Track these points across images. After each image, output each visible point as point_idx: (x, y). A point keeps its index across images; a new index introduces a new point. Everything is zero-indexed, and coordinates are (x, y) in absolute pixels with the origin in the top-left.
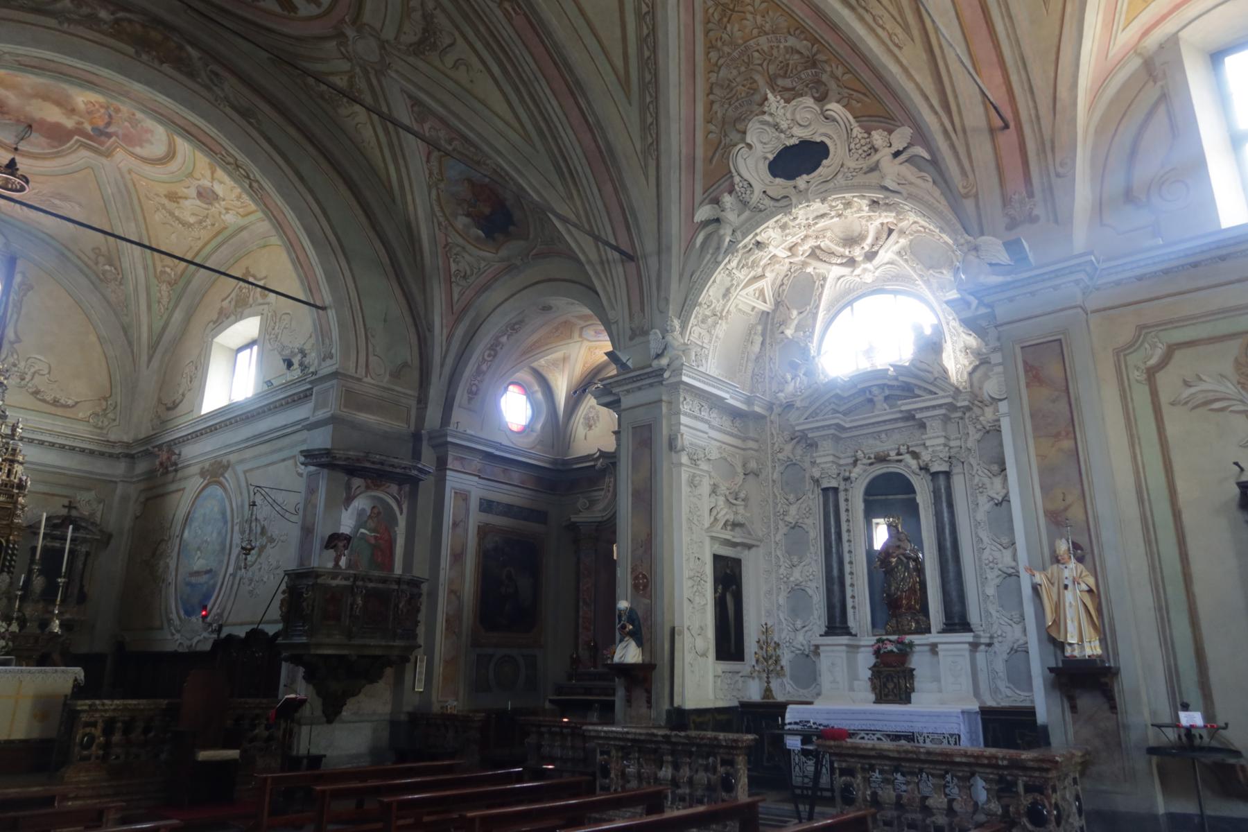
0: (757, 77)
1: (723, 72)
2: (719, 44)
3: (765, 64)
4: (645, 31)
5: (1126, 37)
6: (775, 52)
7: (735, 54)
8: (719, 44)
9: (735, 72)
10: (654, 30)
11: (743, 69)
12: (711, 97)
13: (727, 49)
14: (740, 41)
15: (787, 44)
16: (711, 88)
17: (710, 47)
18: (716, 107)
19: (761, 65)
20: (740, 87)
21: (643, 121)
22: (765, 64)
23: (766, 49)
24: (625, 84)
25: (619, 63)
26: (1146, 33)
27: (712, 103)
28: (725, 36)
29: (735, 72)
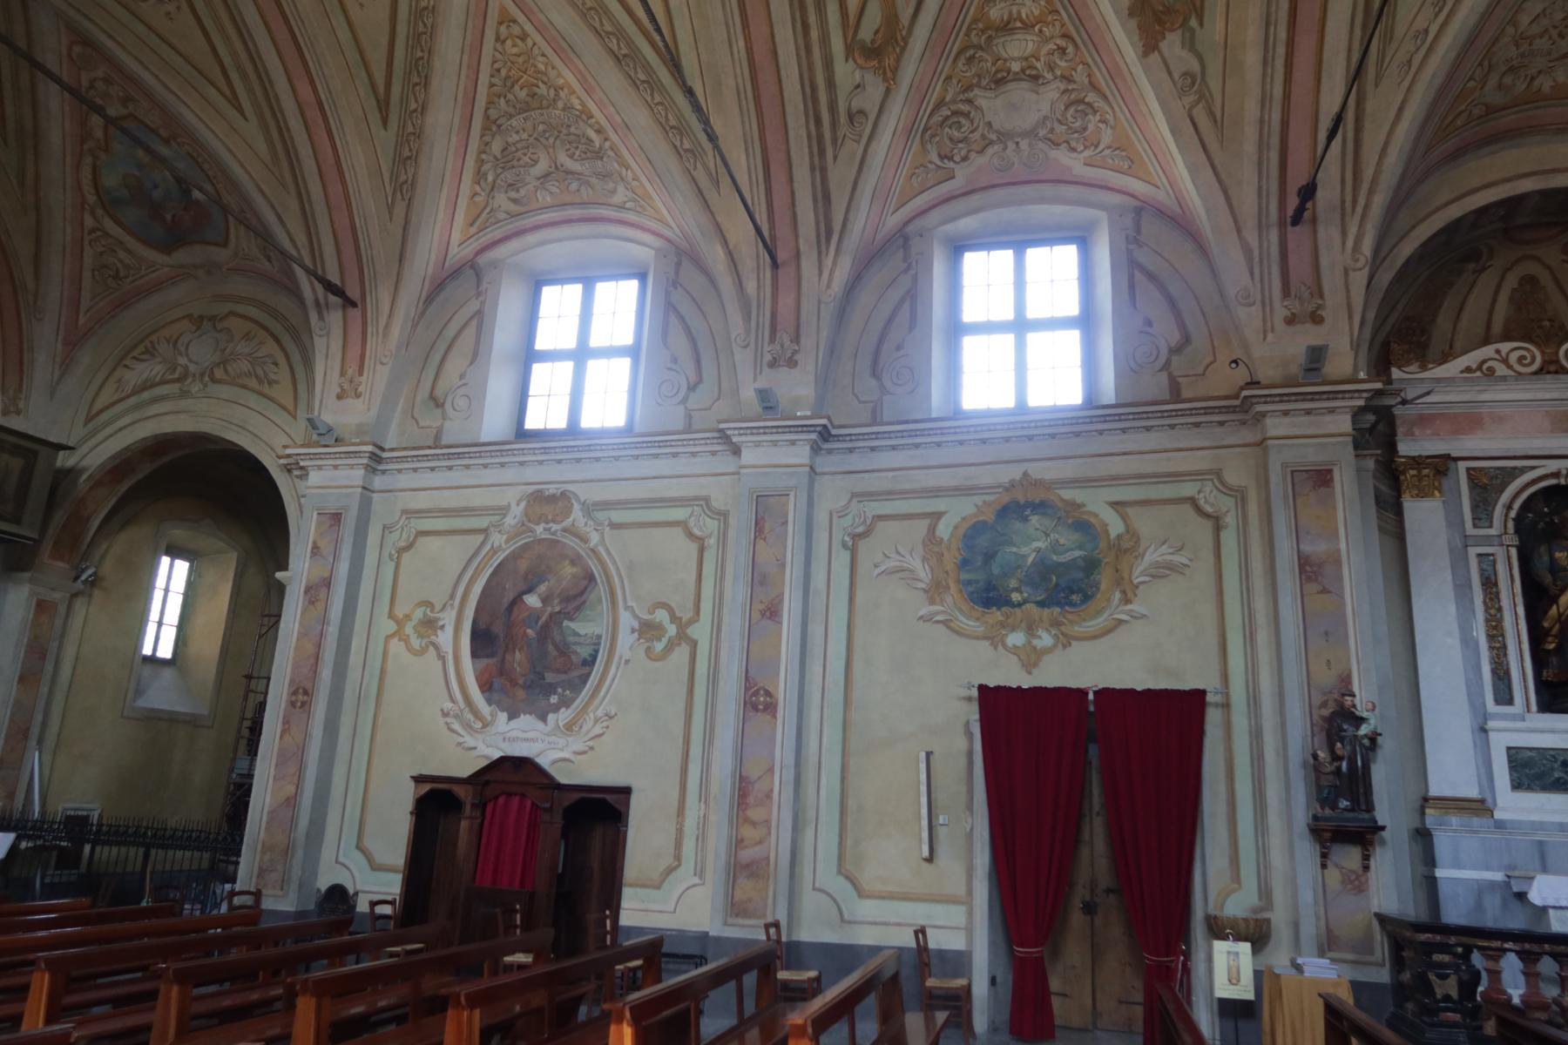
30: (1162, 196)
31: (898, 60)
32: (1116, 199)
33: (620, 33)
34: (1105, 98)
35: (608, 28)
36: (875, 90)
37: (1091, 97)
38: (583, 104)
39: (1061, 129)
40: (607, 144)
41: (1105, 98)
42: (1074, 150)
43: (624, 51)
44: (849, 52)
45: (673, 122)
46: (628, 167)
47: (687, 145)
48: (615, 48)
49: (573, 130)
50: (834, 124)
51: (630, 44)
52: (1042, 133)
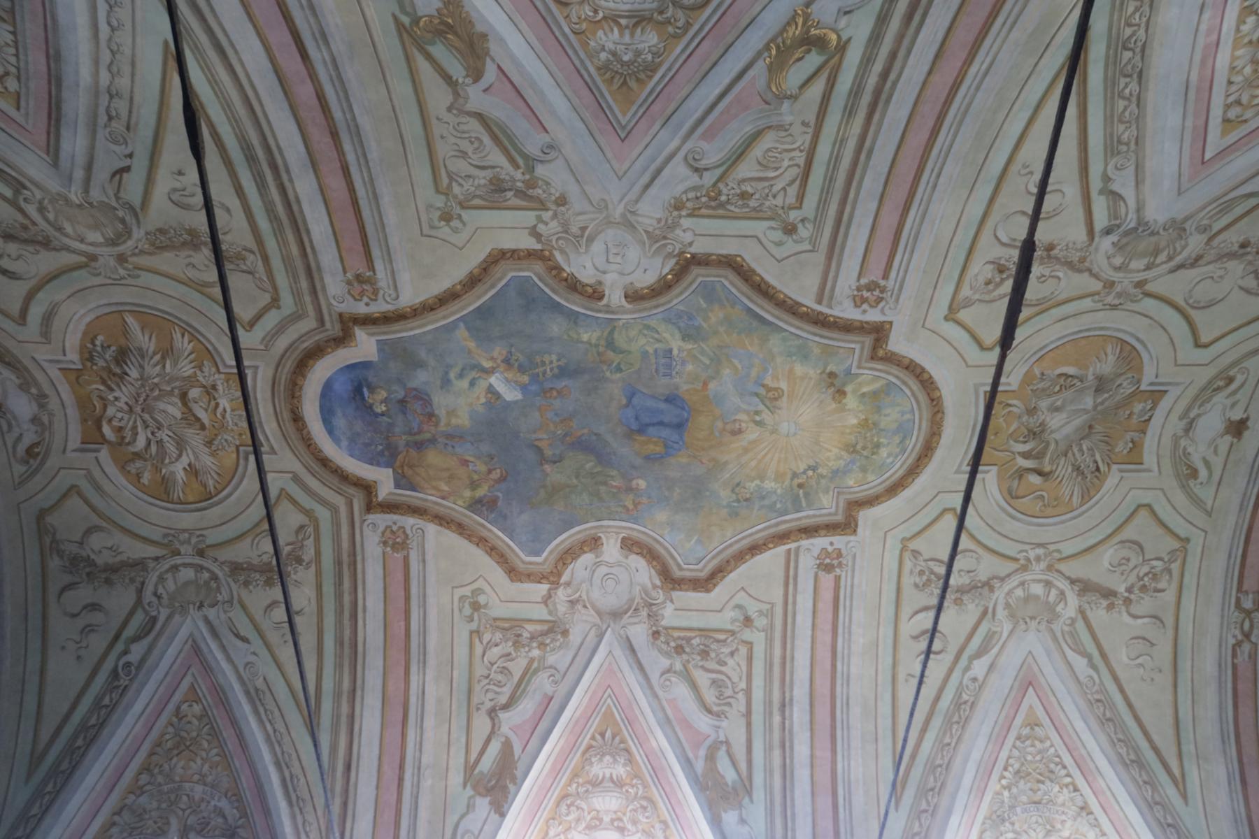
0: (174, 822)
1: (143, 800)
2: (156, 771)
3: (188, 811)
4: (93, 721)
6: (203, 806)
7: (165, 788)
8: (156, 771)
9: (155, 804)
10: (102, 725)
11: (164, 806)
12: (116, 818)
13: (160, 779)
14: (177, 779)
15: (219, 804)
16: (121, 809)
17: (146, 768)
18: (114, 830)
19: (184, 810)
20: (150, 822)
21: (30, 803)
22: (188, 811)
23: (197, 798)
24: (36, 759)
25: (45, 736)
27: (114, 824)
28: (166, 766)
29: (155, 804)
31: (784, 30)
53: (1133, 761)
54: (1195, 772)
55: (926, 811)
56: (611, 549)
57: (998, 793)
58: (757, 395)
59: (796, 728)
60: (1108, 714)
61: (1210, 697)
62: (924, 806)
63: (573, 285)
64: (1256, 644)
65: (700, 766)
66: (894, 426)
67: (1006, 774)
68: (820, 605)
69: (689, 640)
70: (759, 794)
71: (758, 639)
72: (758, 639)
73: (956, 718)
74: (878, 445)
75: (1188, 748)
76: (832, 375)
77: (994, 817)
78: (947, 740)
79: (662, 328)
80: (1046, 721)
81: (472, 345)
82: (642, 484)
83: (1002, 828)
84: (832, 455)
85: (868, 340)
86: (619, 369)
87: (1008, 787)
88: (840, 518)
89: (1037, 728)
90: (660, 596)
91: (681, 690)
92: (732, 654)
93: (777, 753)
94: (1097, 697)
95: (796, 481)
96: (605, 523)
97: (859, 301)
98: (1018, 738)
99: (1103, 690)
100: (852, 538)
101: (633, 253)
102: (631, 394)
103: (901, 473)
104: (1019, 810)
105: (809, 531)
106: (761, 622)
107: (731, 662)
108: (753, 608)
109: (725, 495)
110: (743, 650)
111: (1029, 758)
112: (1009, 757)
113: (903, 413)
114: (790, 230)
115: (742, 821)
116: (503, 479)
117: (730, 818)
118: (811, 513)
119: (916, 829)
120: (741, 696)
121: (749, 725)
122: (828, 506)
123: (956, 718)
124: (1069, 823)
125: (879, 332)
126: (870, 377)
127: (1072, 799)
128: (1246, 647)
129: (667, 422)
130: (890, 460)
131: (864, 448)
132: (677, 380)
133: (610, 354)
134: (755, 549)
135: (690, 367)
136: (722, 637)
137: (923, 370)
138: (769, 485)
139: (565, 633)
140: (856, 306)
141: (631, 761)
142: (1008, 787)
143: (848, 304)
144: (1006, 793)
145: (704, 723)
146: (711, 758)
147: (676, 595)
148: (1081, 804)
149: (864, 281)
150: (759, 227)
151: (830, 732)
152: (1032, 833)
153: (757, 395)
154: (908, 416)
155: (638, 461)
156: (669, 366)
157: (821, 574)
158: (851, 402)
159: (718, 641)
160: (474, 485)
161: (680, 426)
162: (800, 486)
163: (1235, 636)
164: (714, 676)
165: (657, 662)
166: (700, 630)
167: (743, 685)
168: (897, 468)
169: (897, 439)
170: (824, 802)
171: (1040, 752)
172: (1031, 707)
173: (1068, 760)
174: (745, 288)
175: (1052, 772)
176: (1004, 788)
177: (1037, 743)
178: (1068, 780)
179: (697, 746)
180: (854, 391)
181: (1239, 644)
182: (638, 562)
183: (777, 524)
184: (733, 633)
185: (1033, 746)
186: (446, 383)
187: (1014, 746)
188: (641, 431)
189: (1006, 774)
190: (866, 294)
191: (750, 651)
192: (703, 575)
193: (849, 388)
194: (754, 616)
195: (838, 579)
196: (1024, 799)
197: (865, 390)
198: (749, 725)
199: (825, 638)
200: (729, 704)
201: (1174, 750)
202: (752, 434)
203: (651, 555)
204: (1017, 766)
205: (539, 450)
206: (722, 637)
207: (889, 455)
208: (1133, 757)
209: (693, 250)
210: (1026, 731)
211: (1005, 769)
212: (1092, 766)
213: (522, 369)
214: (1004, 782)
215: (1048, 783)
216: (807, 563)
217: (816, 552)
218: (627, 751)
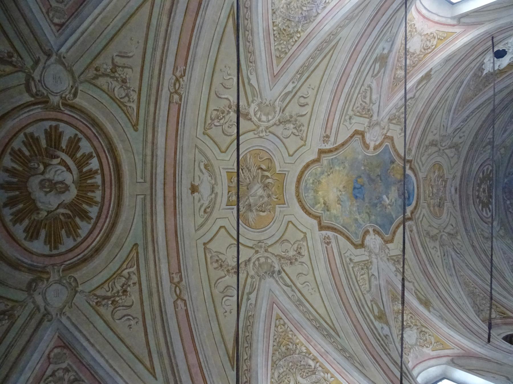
5: (457, 30)
17: (476, 95)
26: (454, 25)
30: (456, 351)
32: (445, 360)
33: (316, 320)
34: (427, 328)
35: (312, 318)
36: (386, 328)
37: (424, 329)
38: (307, 349)
39: (422, 341)
40: (318, 364)
41: (427, 328)
42: (427, 347)
43: (318, 325)
44: (375, 319)
45: (340, 348)
46: (327, 372)
47: (348, 355)
48: (315, 324)
49: (302, 363)
50: (383, 340)
51: (319, 323)
52: (418, 344)
53: (248, 31)
54: (222, 16)
55: (333, 35)
56: (372, 146)
57: (303, 31)
58: (342, 201)
59: (353, 77)
60: (249, 55)
61: (201, 51)
62: (332, 37)
63: (378, 233)
64: (173, 74)
65: (383, 70)
66: (310, 191)
67: (297, 39)
68: (331, 122)
69: (365, 114)
70: (374, 56)
71: (350, 113)
72: (350, 113)
73: (305, 68)
74: (313, 183)
75: (220, 29)
76: (328, 211)
77: (308, 21)
78: (312, 60)
79: (361, 222)
80: (274, 58)
81: (392, 213)
82: (363, 168)
83: (307, 14)
84: (324, 180)
85: (322, 224)
86: (367, 206)
87: (298, 32)
88: (323, 155)
89: (278, 56)
90: (366, 130)
91: (374, 97)
92: (358, 107)
93: (362, 70)
94: (251, 64)
95: (332, 170)
96: (371, 155)
97: (328, 238)
98: (286, 53)
99: (248, 66)
100: (320, 148)
101: (372, 246)
102: (363, 199)
103: (306, 172)
104: (297, 20)
105: (330, 151)
106: (347, 117)
107: (359, 105)
108: (347, 124)
109: (347, 165)
110: (354, 108)
111: (285, 43)
112: (293, 46)
113: (308, 196)
114: (351, 260)
115: (384, 49)
116: (388, 170)
117: (386, 51)
118: (329, 158)
119: (340, 29)
120: (361, 92)
121: (364, 81)
122: (325, 160)
123: (305, 68)
124: (281, 6)
125: (322, 228)
126: (318, 210)
127: (276, 18)
128: (178, 74)
129: (357, 191)
130: (309, 178)
131: (316, 182)
132: (356, 204)
133: (368, 211)
134: (343, 145)
135: (354, 209)
136: (358, 114)
137: (305, 213)
138: (337, 168)
139: (389, 119)
140: (328, 236)
141: (395, 75)
142: (298, 32)
143: (331, 236)
144: (299, 30)
145: (374, 86)
146: (379, 72)
147: (362, 130)
148: (274, 15)
149: (330, 245)
150: (356, 259)
151: (344, 73)
152: (295, 5)
153: (342, 201)
154: (306, 195)
155: (362, 175)
156: (358, 209)
157: (329, 135)
158: (322, 201)
159: (358, 112)
160: (393, 168)
161: (355, 188)
162: (331, 168)
163: (183, 81)
164: (365, 100)
165: (375, 108)
166: (361, 116)
167: (359, 95)
168: (307, 174)
169: (308, 186)
170: (359, 48)
171: (280, 44)
172: (277, 66)
173: (272, 38)
174: (351, 238)
175: (279, 34)
176: (299, 33)
177: (280, 49)
178: (275, 28)
179: (380, 77)
180: (321, 205)
181: (182, 76)
182: (368, 141)
183: (338, 153)
184: (355, 115)
185: (282, 48)
186: (396, 201)
187: (289, 50)
188: (362, 186)
189: (297, 39)
190: (328, 240)
191: (353, 107)
192: (356, 136)
193: (323, 205)
194: (348, 120)
195: (325, 132)
196: (293, 24)
197: (319, 205)
198: (364, 81)
199: (333, 109)
200: (365, 89)
201: (227, 30)
202: (341, 186)
203: (364, 143)
204: (291, 41)
205: (381, 179)
206: (358, 114)
207: (309, 180)
208: (247, 33)
209: (363, 249)
210: (282, 56)
211: (296, 41)
212: (265, 34)
213: (383, 205)
214: (299, 35)
215: (282, 29)
216: (332, 139)
217: (329, 143)
218: (394, 79)
